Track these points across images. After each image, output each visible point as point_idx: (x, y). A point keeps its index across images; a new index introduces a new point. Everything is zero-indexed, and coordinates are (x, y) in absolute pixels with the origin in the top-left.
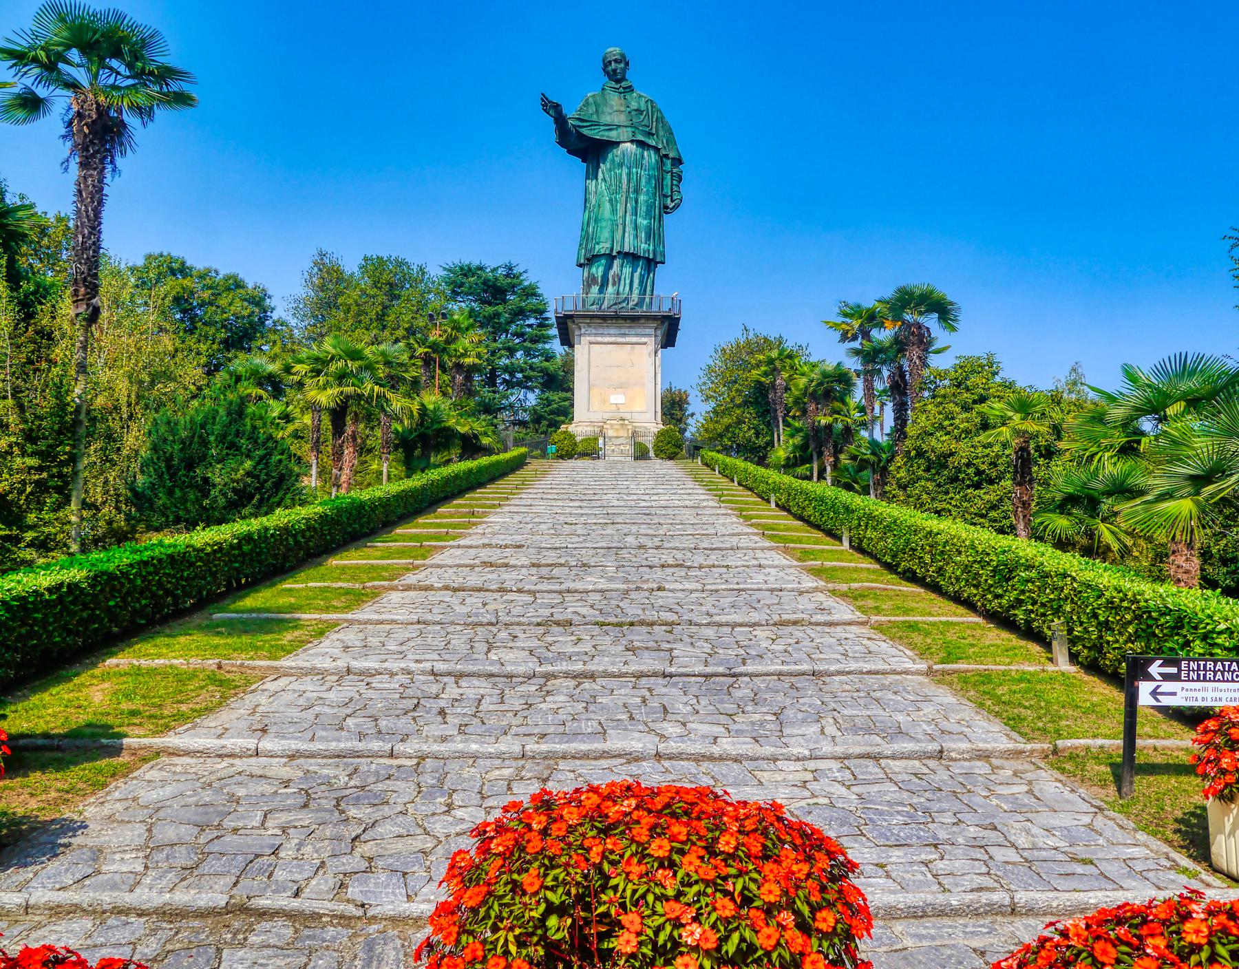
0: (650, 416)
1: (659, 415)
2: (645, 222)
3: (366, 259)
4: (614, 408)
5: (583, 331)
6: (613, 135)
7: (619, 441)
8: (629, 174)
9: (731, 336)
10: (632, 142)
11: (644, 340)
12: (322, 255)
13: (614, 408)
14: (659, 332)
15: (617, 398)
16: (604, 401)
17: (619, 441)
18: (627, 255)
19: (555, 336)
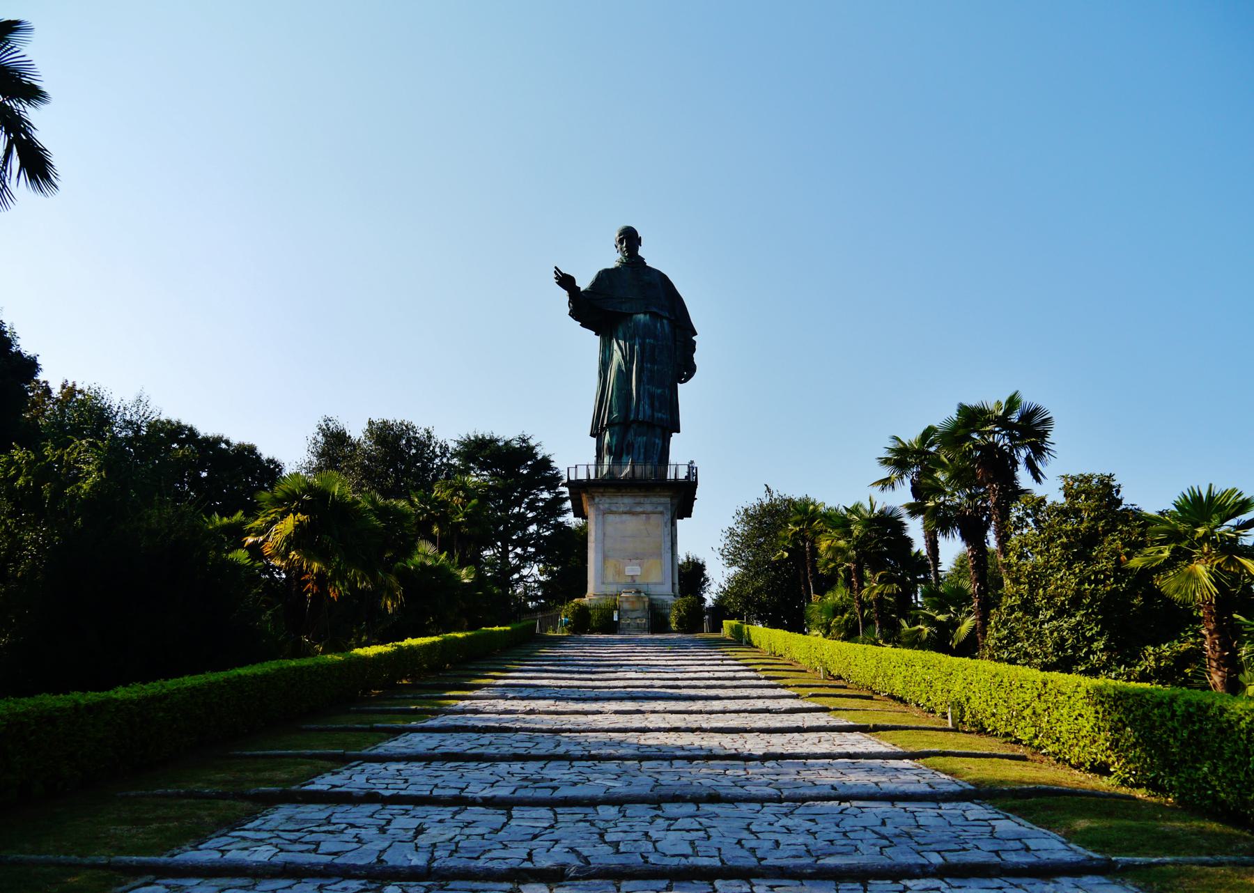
0: (667, 588)
1: (677, 587)
2: (659, 391)
3: (371, 423)
4: (629, 580)
5: (597, 500)
6: (625, 308)
7: (635, 615)
8: (642, 346)
9: (753, 497)
10: (645, 313)
11: (660, 509)
12: (327, 420)
13: (629, 580)
14: (675, 501)
15: (632, 570)
16: (619, 572)
17: (635, 615)
18: (641, 423)
19: (569, 510)
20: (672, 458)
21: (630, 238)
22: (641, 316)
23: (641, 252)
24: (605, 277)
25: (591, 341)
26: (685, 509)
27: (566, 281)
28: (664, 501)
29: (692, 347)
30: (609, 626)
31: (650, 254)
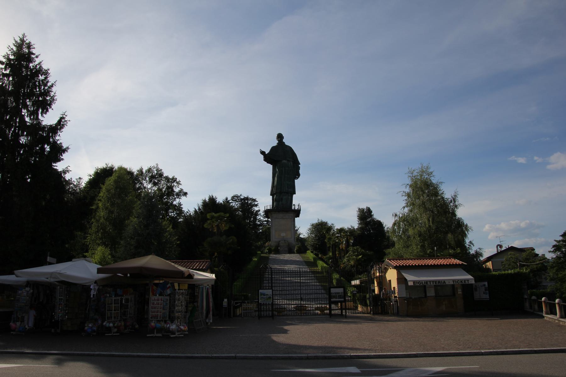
15: (283, 234)
20: (294, 203)
21: (280, 137)
22: (284, 161)
23: (284, 141)
24: (273, 149)
25: (270, 167)
26: (298, 216)
27: (263, 153)
28: (292, 215)
29: (299, 168)
30: (277, 251)
31: (286, 141)
